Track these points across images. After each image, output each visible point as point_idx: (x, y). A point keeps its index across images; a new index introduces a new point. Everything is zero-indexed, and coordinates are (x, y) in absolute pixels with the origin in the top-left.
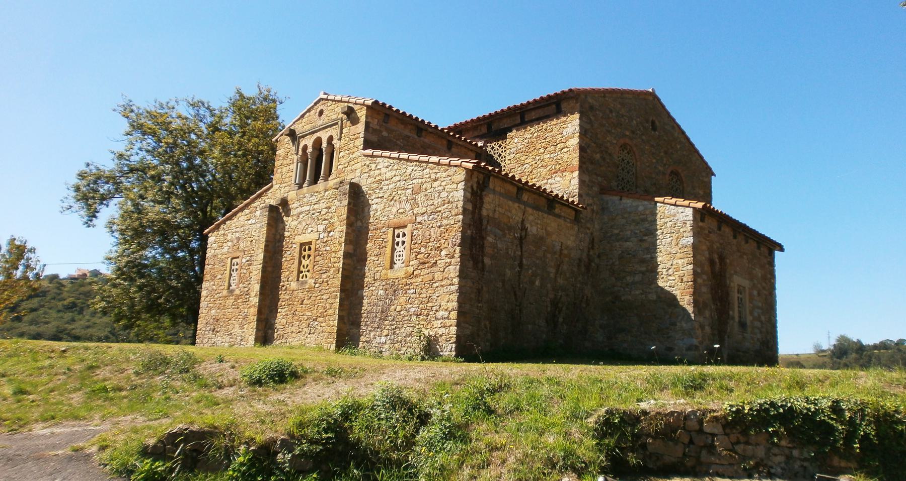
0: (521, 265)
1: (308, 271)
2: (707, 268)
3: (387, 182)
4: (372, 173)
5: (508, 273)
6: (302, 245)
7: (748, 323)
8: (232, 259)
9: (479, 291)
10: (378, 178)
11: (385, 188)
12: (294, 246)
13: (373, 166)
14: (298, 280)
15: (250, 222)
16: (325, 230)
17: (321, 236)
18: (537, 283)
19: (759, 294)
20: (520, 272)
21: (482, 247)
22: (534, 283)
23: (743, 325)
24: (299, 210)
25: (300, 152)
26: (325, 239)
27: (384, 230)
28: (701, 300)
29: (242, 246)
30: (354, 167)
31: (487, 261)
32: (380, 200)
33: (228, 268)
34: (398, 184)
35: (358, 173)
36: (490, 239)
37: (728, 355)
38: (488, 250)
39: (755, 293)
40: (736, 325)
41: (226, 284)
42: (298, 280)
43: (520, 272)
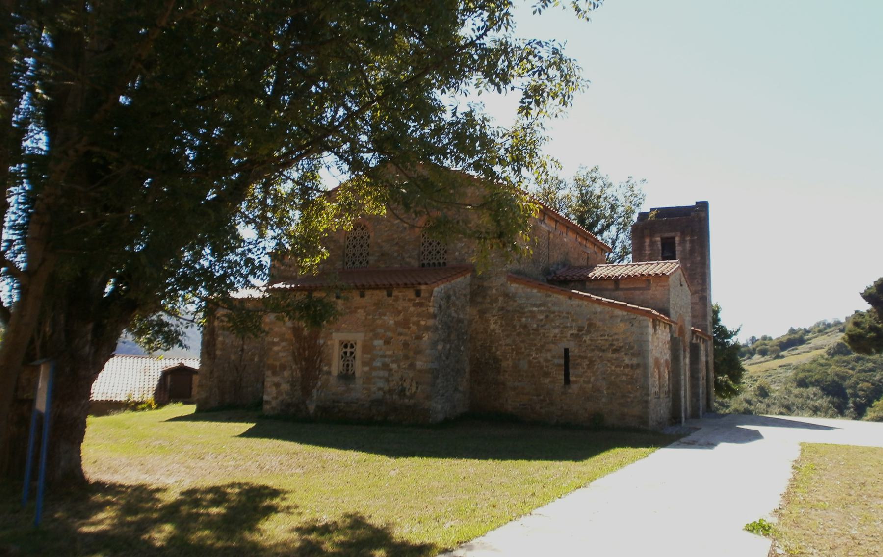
0: (242, 350)
2: (289, 335)
5: (233, 357)
7: (357, 374)
9: (212, 372)
18: (256, 360)
19: (387, 342)
20: (241, 356)
21: (215, 345)
22: (252, 360)
23: (347, 376)
28: (278, 363)
31: (218, 352)
36: (220, 339)
37: (318, 406)
38: (219, 346)
39: (378, 343)
40: (333, 381)
43: (241, 356)
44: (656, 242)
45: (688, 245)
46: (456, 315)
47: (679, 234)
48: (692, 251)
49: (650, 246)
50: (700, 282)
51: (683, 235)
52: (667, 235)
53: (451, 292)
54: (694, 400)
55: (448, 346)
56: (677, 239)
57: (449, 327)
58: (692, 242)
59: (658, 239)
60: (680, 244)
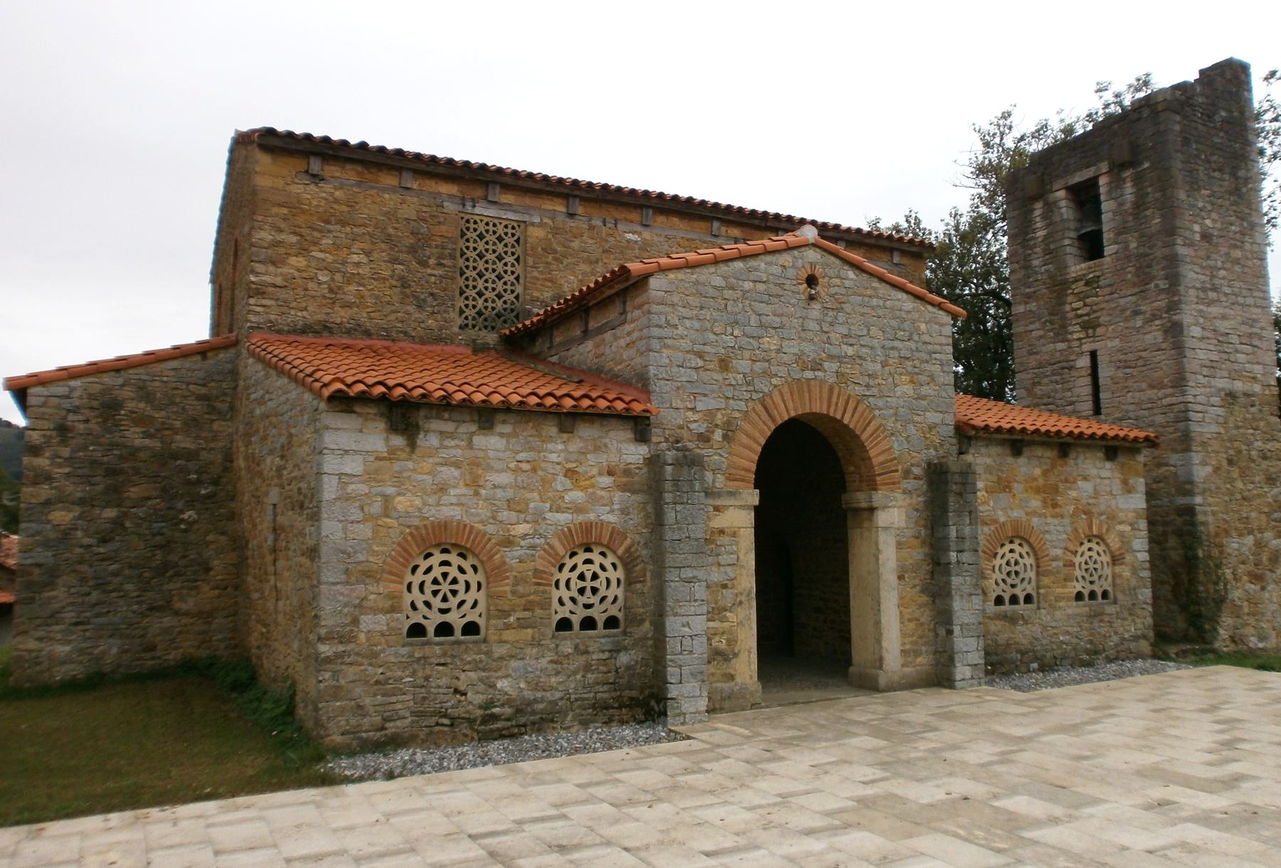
44: (1056, 202)
45: (1129, 188)
46: (156, 444)
47: (1104, 167)
48: (1139, 205)
49: (1045, 217)
50: (1163, 284)
51: (1117, 168)
52: (1078, 178)
53: (127, 393)
54: (942, 632)
55: (110, 513)
56: (1103, 181)
57: (112, 472)
58: (1138, 180)
59: (1062, 194)
60: (1109, 192)
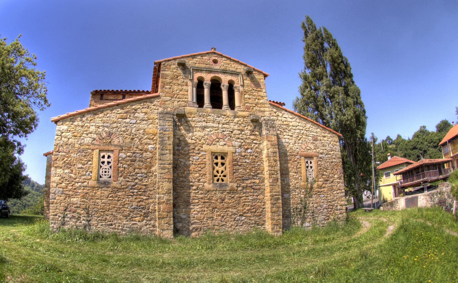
1: (225, 176)
3: (294, 128)
4: (279, 118)
6: (213, 153)
8: (100, 151)
10: (285, 123)
11: (292, 130)
12: (202, 153)
13: (280, 115)
14: (213, 182)
15: (128, 120)
16: (240, 146)
17: (237, 150)
24: (204, 124)
25: (196, 81)
26: (243, 154)
27: (298, 157)
29: (116, 141)
30: (262, 109)
32: (290, 138)
33: (95, 159)
34: (302, 132)
35: (267, 113)
41: (94, 175)
42: (213, 182)
